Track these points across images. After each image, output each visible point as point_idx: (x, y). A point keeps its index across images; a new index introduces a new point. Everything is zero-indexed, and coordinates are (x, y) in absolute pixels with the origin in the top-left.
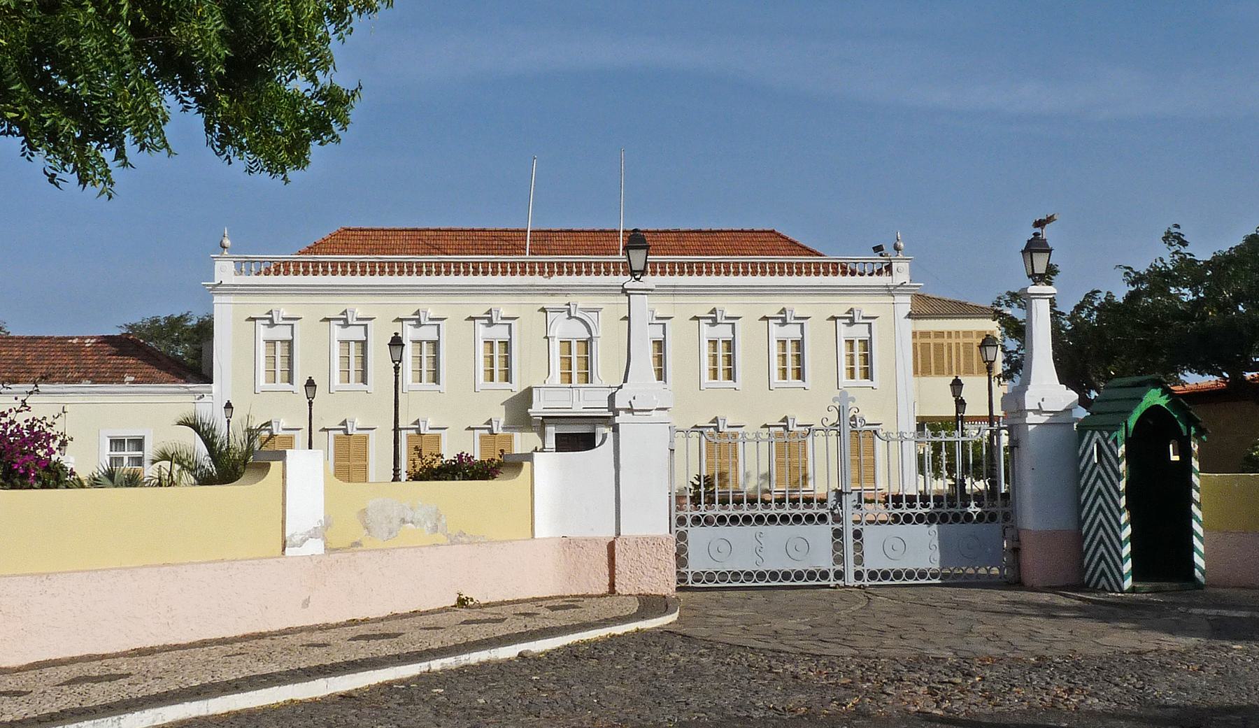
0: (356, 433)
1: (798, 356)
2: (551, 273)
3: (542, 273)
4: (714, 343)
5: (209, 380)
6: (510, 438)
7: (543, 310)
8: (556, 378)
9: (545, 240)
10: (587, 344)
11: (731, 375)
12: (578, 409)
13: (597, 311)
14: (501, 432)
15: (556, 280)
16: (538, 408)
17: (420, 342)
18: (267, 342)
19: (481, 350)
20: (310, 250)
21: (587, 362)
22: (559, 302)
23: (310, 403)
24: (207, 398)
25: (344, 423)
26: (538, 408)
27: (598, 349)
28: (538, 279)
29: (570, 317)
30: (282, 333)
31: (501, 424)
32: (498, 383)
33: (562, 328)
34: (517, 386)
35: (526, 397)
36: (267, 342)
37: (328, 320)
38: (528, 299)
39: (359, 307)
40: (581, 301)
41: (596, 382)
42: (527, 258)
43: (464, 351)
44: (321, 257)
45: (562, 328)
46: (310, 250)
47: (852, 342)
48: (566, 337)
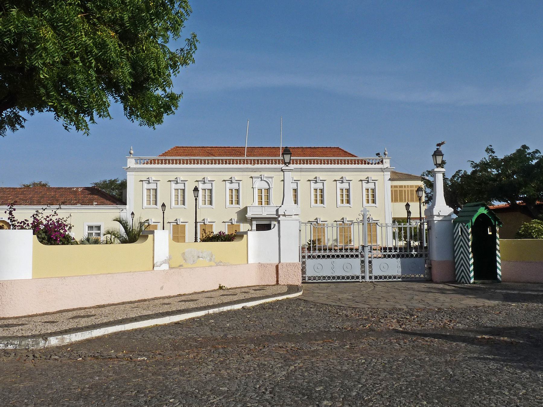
0: (181, 224)
1: (348, 195)
2: (254, 164)
3: (251, 163)
4: (316, 190)
5: (126, 205)
6: (239, 226)
7: (251, 177)
8: (256, 203)
9: (252, 151)
10: (268, 190)
11: (322, 202)
12: (264, 215)
13: (272, 178)
14: (235, 223)
15: (256, 166)
16: (249, 215)
17: (205, 190)
18: (147, 189)
19: (228, 192)
20: (164, 155)
21: (268, 197)
22: (257, 174)
23: (164, 213)
24: (124, 211)
25: (176, 220)
26: (249, 215)
27: (272, 192)
28: (249, 166)
29: (262, 180)
30: (153, 186)
31: (236, 221)
32: (234, 205)
33: (259, 184)
34: (242, 206)
35: (245, 210)
36: (147, 189)
37: (170, 181)
38: (245, 173)
39: (182, 176)
40: (266, 174)
41: (272, 205)
42: (245, 158)
43: (221, 194)
44: (167, 158)
45: (259, 184)
46: (164, 155)
47: (368, 190)
48: (260, 187)
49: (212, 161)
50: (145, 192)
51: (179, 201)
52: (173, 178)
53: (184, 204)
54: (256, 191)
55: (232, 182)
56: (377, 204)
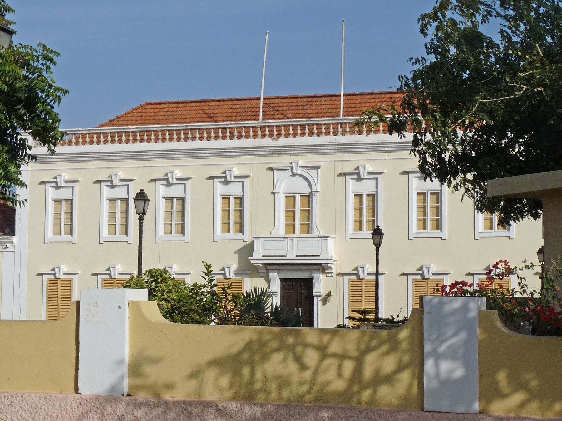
0: (432, 277)
1: (438, 207)
2: (279, 135)
3: (271, 136)
4: (359, 196)
5: (13, 233)
6: (241, 283)
7: (270, 169)
8: (281, 230)
9: (278, 107)
10: (308, 197)
11: (438, 226)
12: (291, 256)
13: (317, 168)
14: (233, 277)
15: (283, 141)
16: (257, 256)
17: (171, 199)
18: (166, 199)
19: (351, 201)
20: (111, 123)
21: (308, 213)
22: (283, 161)
23: (377, 250)
24: (10, 248)
25: (421, 268)
26: (257, 256)
27: (317, 201)
28: (267, 142)
29: (294, 175)
30: (367, 186)
31: (232, 271)
32: (233, 235)
33: (286, 184)
34: (247, 237)
35: (249, 249)
36: (166, 199)
37: (344, 174)
38: (256, 160)
39: (121, 172)
40: (302, 160)
41: (315, 233)
42: (261, 122)
43: (206, 206)
44: (221, 124)
45: (286, 184)
46: (111, 123)
47: (360, 196)
48: (291, 191)
49: (171, 135)
50: (51, 206)
51: (118, 227)
52: (217, 172)
53: (183, 232)
54: (281, 201)
55: (359, 179)
56: (188, 236)
